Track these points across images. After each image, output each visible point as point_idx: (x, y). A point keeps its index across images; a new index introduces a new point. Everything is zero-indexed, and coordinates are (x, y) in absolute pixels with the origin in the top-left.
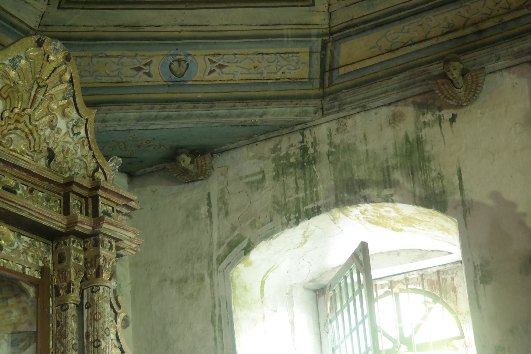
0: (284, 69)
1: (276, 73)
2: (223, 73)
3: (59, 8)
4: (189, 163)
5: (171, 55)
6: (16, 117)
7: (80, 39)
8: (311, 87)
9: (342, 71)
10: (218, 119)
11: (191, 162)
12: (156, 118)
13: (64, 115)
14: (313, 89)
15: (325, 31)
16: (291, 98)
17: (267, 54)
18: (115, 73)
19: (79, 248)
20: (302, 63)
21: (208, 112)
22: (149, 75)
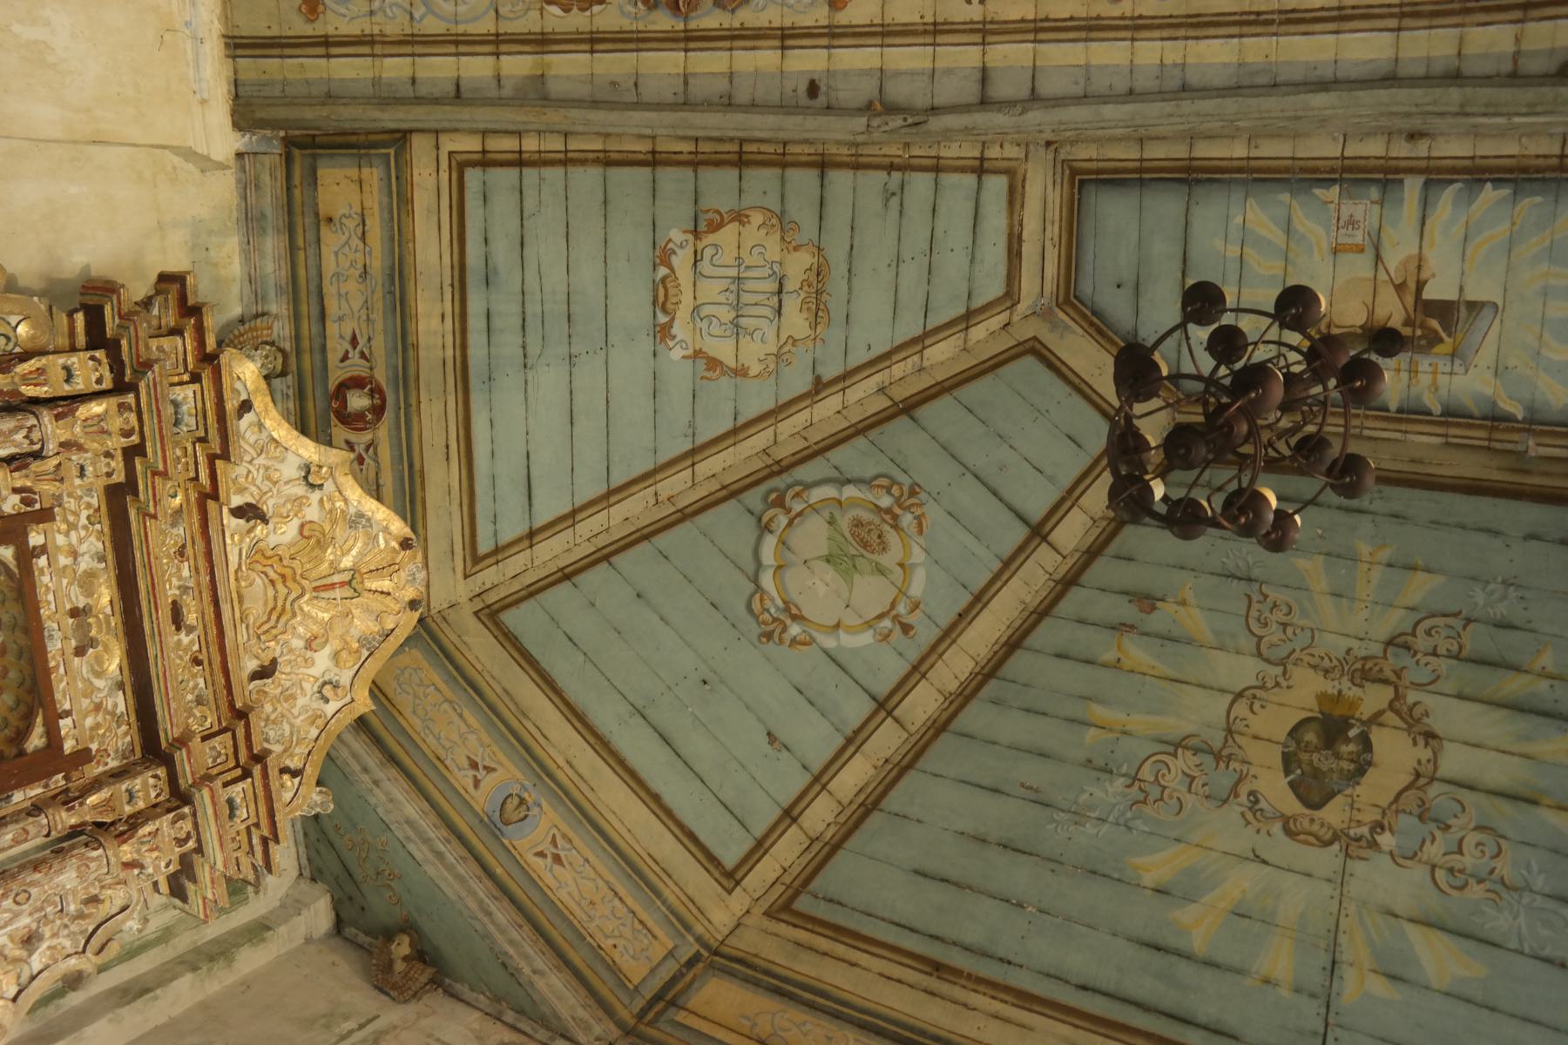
0: (621, 942)
1: (607, 937)
2: (551, 870)
3: (476, 613)
4: (402, 955)
5: (523, 786)
6: (288, 572)
7: (457, 668)
8: (627, 1002)
9: (681, 1017)
10: (486, 920)
11: (405, 959)
12: (427, 841)
13: (336, 656)
14: (626, 1007)
15: (712, 941)
16: (592, 992)
17: (620, 899)
18: (448, 745)
19: (153, 794)
20: (648, 958)
21: (487, 900)
22: (477, 783)
